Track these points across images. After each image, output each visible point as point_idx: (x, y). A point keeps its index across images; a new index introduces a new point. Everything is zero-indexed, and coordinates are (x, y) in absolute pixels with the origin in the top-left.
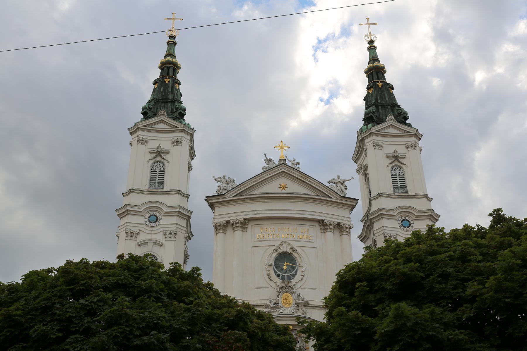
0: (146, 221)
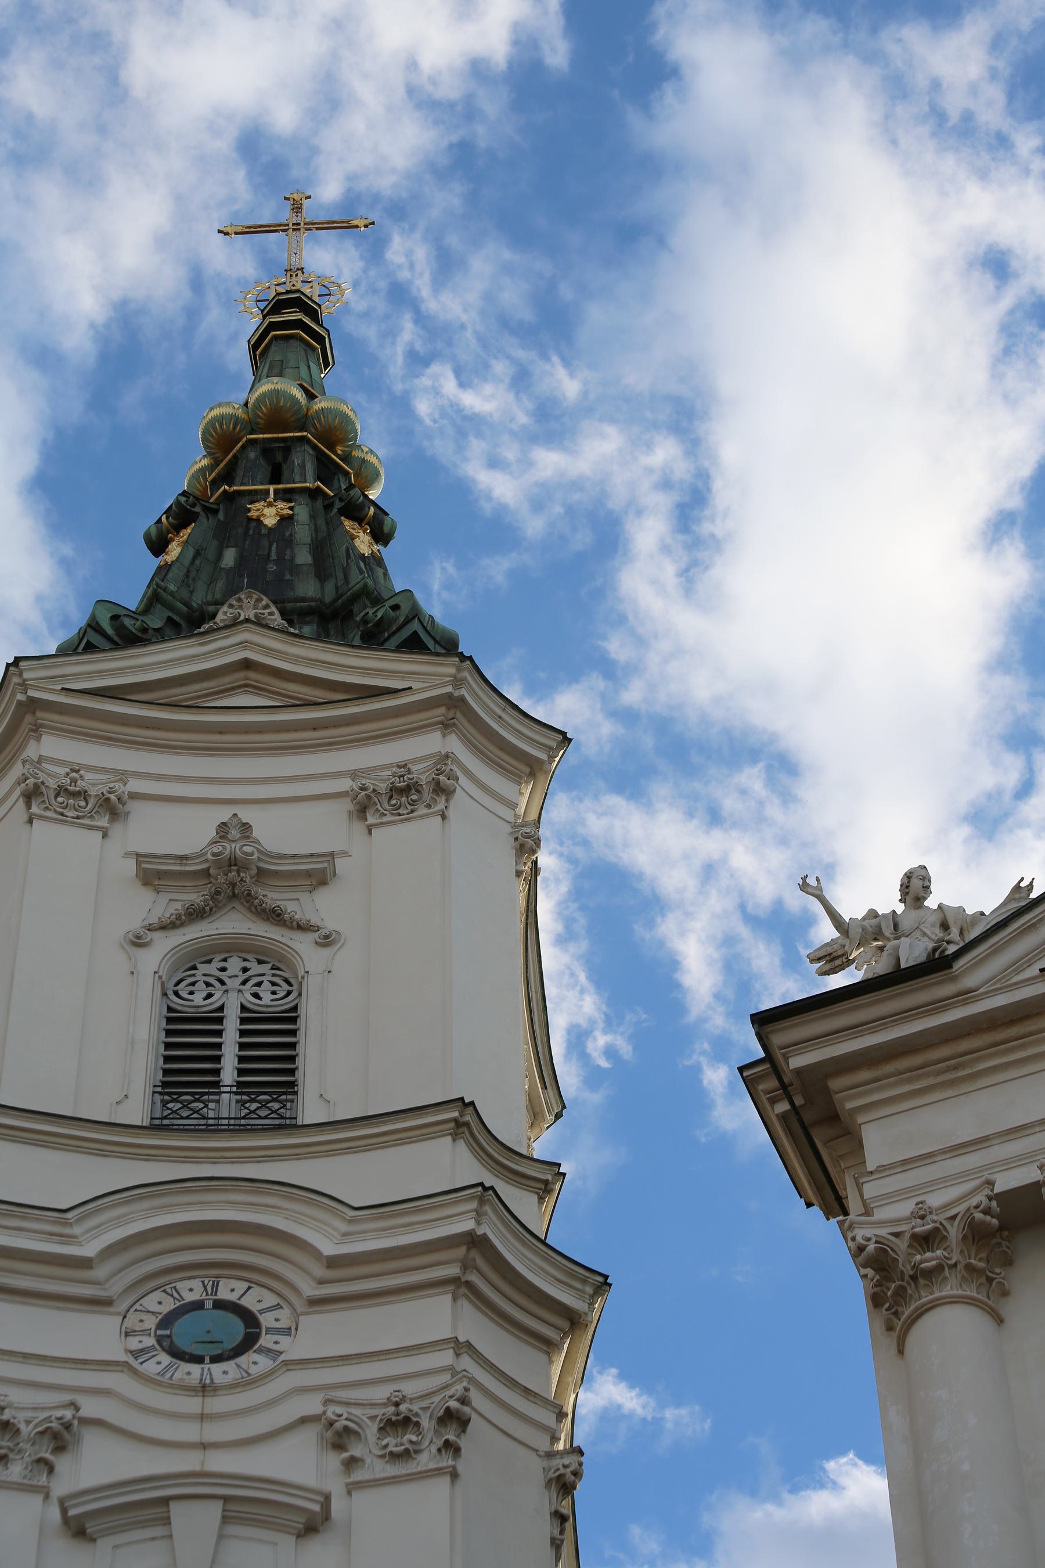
0: (134, 1343)
